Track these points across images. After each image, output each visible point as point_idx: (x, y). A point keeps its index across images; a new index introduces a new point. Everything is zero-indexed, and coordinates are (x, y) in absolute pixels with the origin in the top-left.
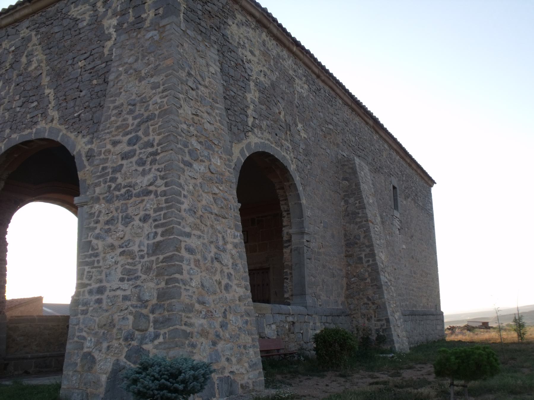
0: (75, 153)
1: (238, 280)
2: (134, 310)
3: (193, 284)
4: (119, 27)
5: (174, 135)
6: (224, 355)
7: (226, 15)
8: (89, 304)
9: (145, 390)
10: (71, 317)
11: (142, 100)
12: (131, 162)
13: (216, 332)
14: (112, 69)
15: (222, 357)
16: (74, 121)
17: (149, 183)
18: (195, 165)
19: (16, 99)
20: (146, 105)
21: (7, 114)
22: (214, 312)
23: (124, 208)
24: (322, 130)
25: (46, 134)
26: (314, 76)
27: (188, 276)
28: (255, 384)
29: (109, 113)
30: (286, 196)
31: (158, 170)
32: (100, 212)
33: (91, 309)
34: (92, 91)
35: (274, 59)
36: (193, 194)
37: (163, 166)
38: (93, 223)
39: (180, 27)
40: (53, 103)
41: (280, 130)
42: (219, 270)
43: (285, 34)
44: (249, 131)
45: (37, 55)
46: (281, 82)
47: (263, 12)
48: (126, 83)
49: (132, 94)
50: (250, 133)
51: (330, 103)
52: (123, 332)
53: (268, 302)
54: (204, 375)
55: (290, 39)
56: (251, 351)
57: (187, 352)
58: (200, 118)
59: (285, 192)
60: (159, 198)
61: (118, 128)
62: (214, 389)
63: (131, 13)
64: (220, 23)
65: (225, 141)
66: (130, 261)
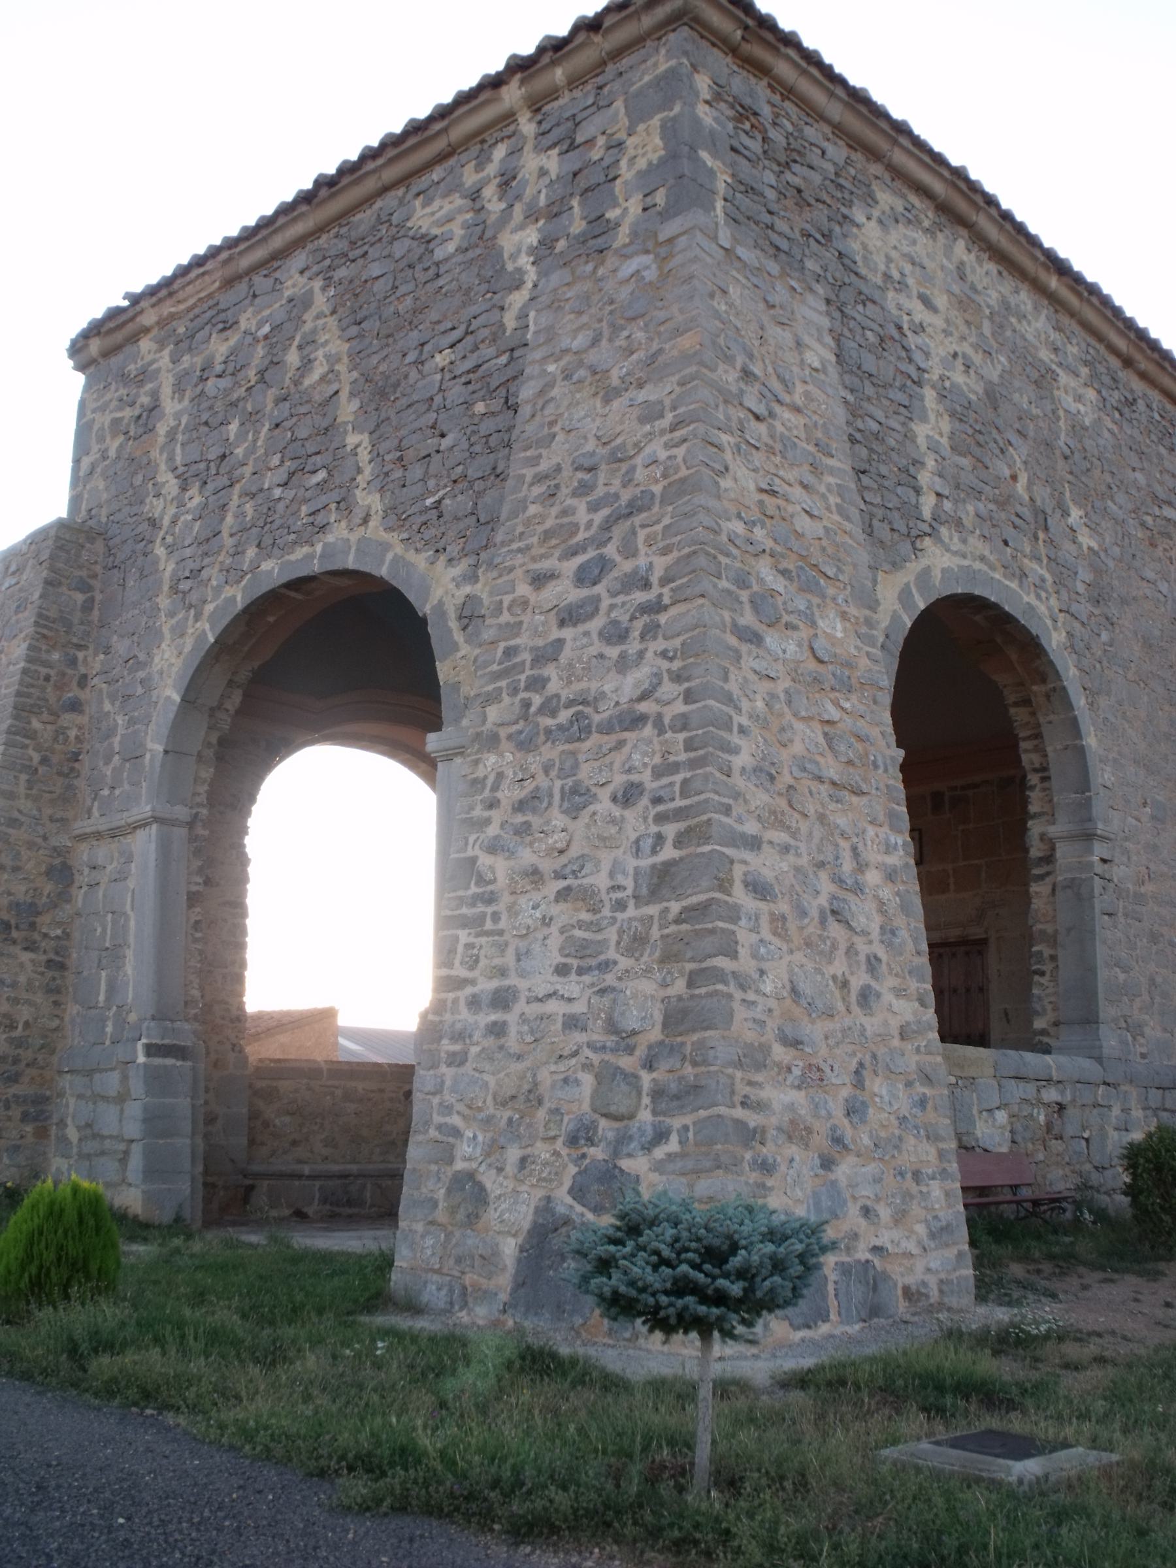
0: (426, 609)
1: (897, 975)
2: (595, 1058)
3: (768, 988)
4: (543, 251)
5: (708, 554)
6: (854, 1198)
7: (847, 196)
8: (470, 1036)
9: (633, 1293)
10: (420, 1072)
11: (613, 453)
12: (587, 634)
13: (834, 1128)
14: (528, 371)
15: (850, 1204)
16: (424, 518)
17: (639, 692)
18: (771, 640)
19: (272, 465)
20: (624, 467)
21: (249, 508)
22: (828, 1070)
23: (568, 765)
24: (1143, 524)
25: (351, 558)
26: (1115, 363)
27: (753, 963)
28: (945, 1288)
29: (522, 494)
30: (1039, 725)
31: (664, 654)
32: (500, 776)
33: (474, 1050)
34: (474, 432)
35: (991, 317)
36: (765, 726)
37: (677, 642)
38: (479, 807)
39: (715, 238)
40: (368, 471)
41: (1015, 527)
42: (843, 946)
43: (1023, 240)
44: (926, 534)
45: (327, 342)
46: (1017, 384)
47: (955, 179)
48: (568, 408)
49: (585, 438)
50: (927, 541)
51: (1167, 441)
52: (566, 1119)
53: (982, 1041)
54: (802, 1257)
55: (1039, 254)
56: (936, 1190)
57: (747, 1183)
58: (780, 502)
59: (1033, 714)
60: (669, 735)
61: (547, 535)
62: (824, 1297)
63: (577, 210)
64: (830, 219)
65: (855, 566)
66: (585, 916)
